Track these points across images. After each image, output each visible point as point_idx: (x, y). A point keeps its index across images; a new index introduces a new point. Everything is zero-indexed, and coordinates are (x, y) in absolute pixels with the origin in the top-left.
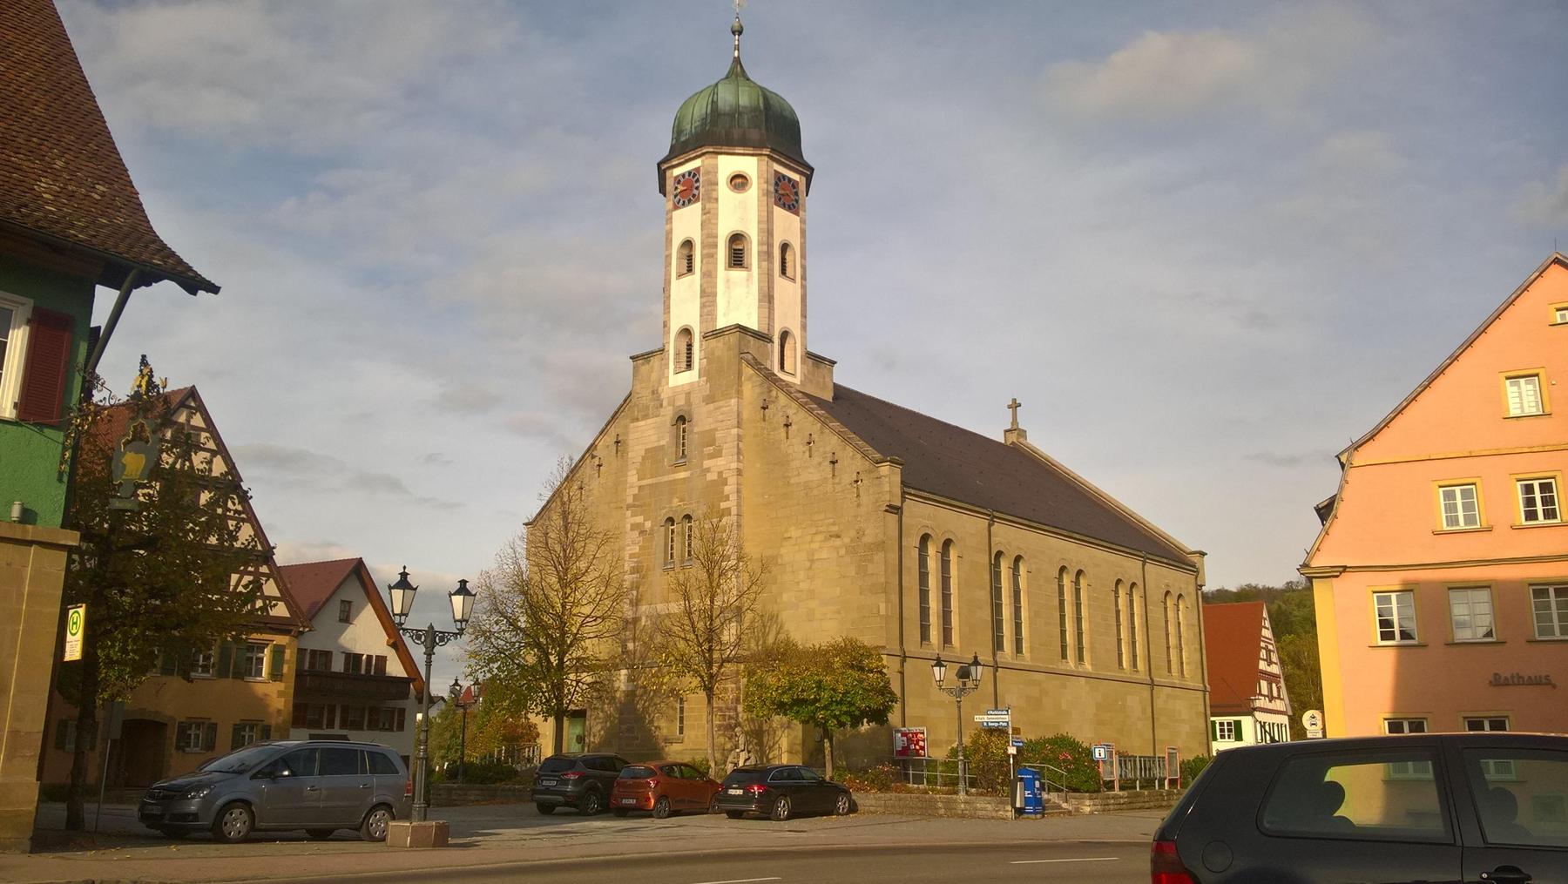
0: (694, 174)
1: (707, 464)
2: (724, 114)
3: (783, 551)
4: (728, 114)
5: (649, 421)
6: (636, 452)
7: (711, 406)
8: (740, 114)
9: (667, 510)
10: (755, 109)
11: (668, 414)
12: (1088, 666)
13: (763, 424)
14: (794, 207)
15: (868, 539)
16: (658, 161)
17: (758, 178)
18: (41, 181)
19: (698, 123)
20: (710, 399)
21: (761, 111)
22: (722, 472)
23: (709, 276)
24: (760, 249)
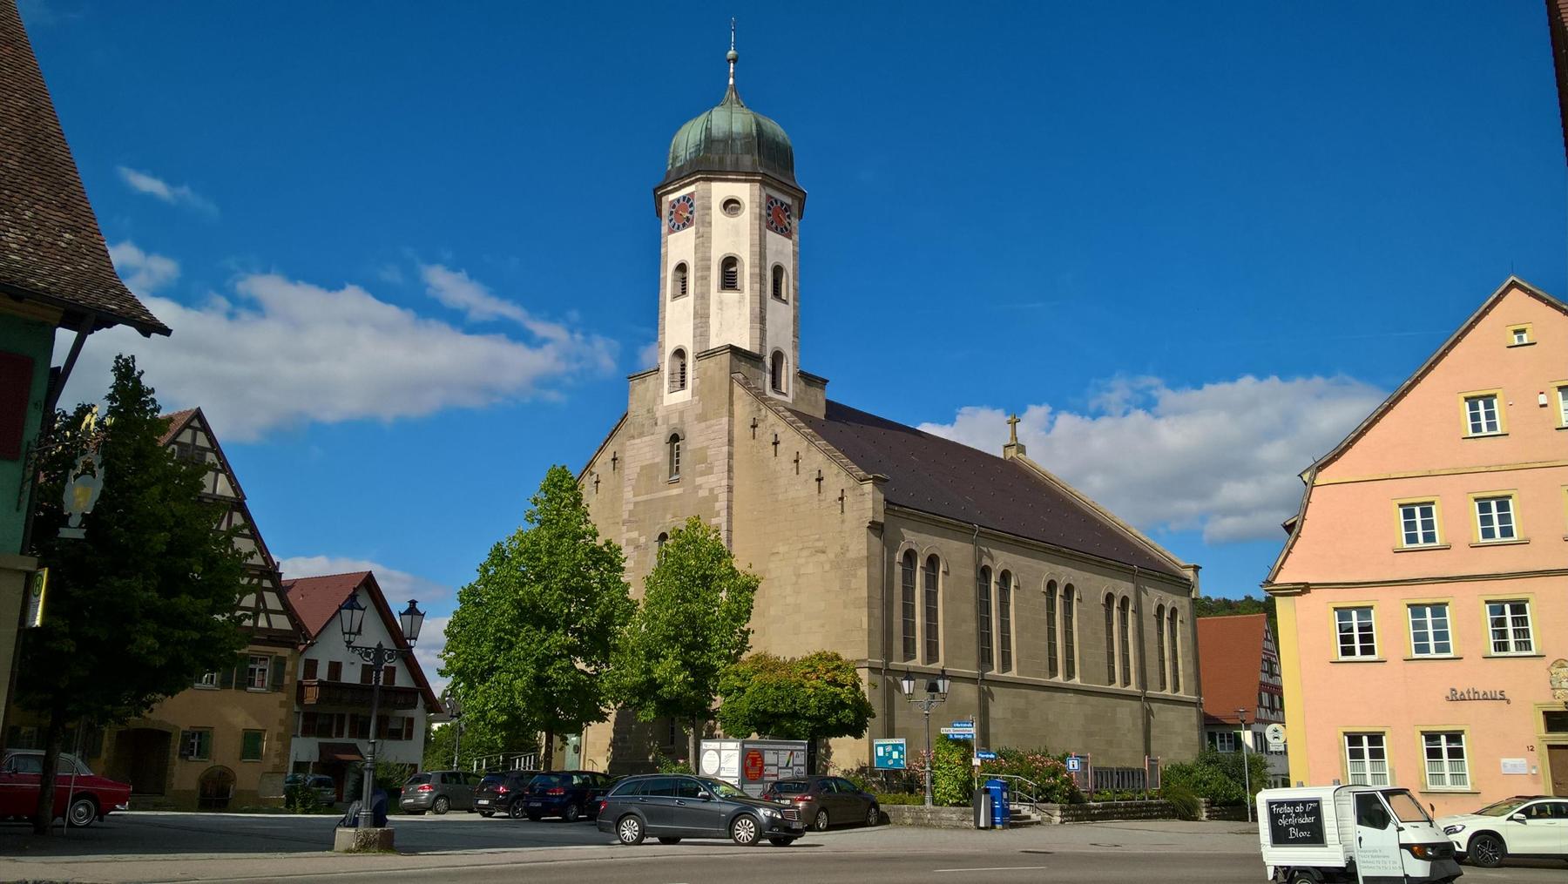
0: (688, 199)
1: (699, 481)
2: (718, 141)
3: (772, 566)
4: (722, 141)
6: (631, 468)
7: (703, 424)
8: (733, 140)
9: (661, 525)
10: (749, 135)
11: (663, 433)
12: (1077, 680)
13: (753, 442)
14: (787, 230)
15: (850, 555)
17: (751, 202)
18: (9, 232)
19: (692, 150)
20: (702, 418)
21: (753, 136)
23: (703, 297)
24: (753, 272)
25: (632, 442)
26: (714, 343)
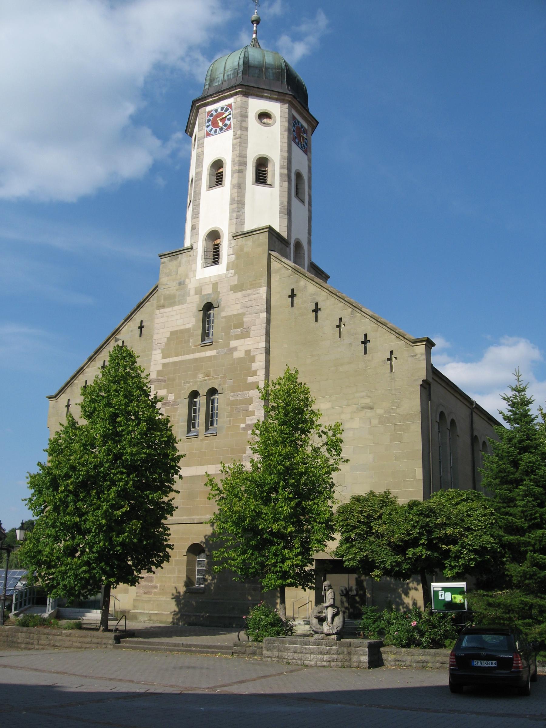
1: (233, 343)
5: (175, 308)
7: (239, 294)
8: (266, 68)
16: (195, 98)
19: (229, 73)
20: (235, 289)
22: (249, 351)
23: (240, 187)
24: (282, 172)
25: (162, 310)
26: (247, 228)
